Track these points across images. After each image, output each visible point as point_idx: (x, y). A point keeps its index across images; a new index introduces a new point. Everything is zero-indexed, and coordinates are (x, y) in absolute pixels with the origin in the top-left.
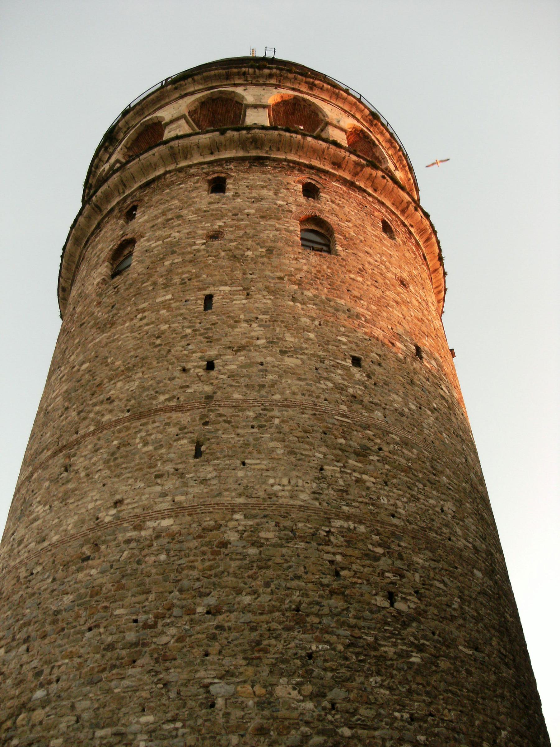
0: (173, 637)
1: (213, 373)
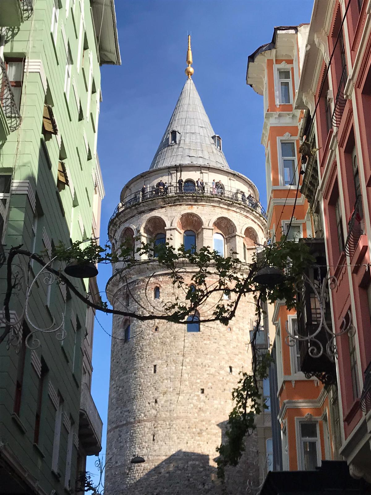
1: (157, 405)
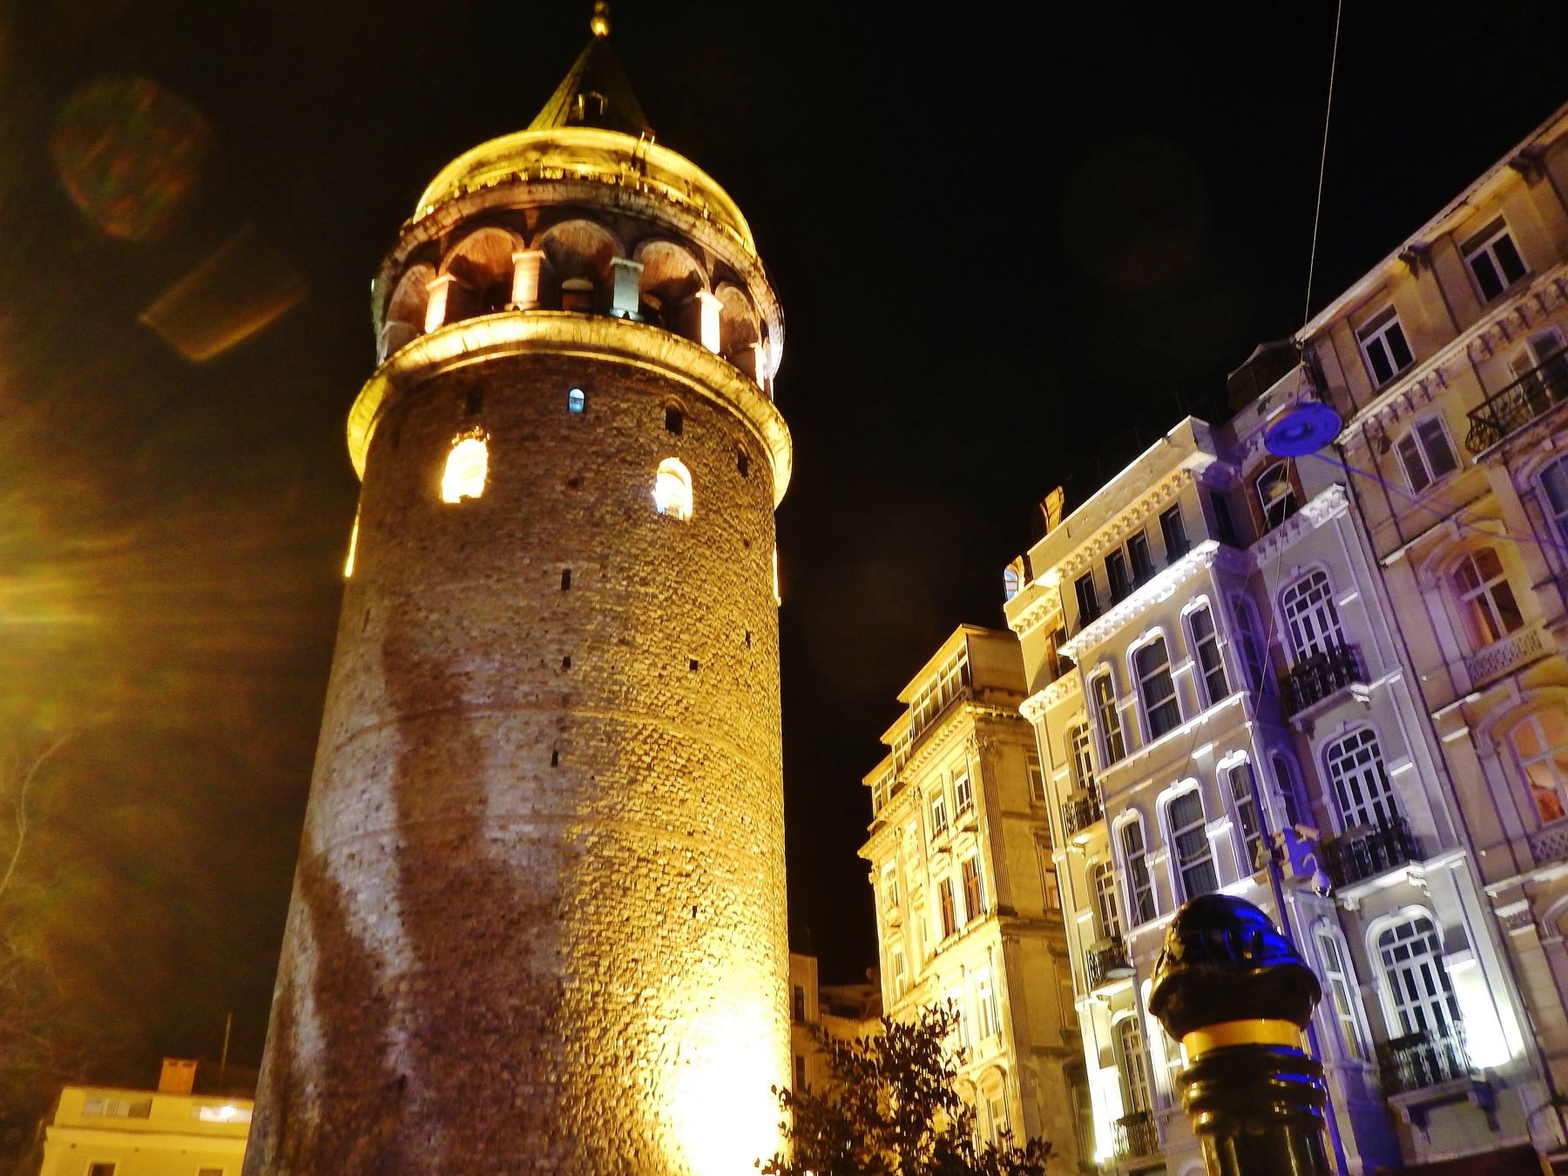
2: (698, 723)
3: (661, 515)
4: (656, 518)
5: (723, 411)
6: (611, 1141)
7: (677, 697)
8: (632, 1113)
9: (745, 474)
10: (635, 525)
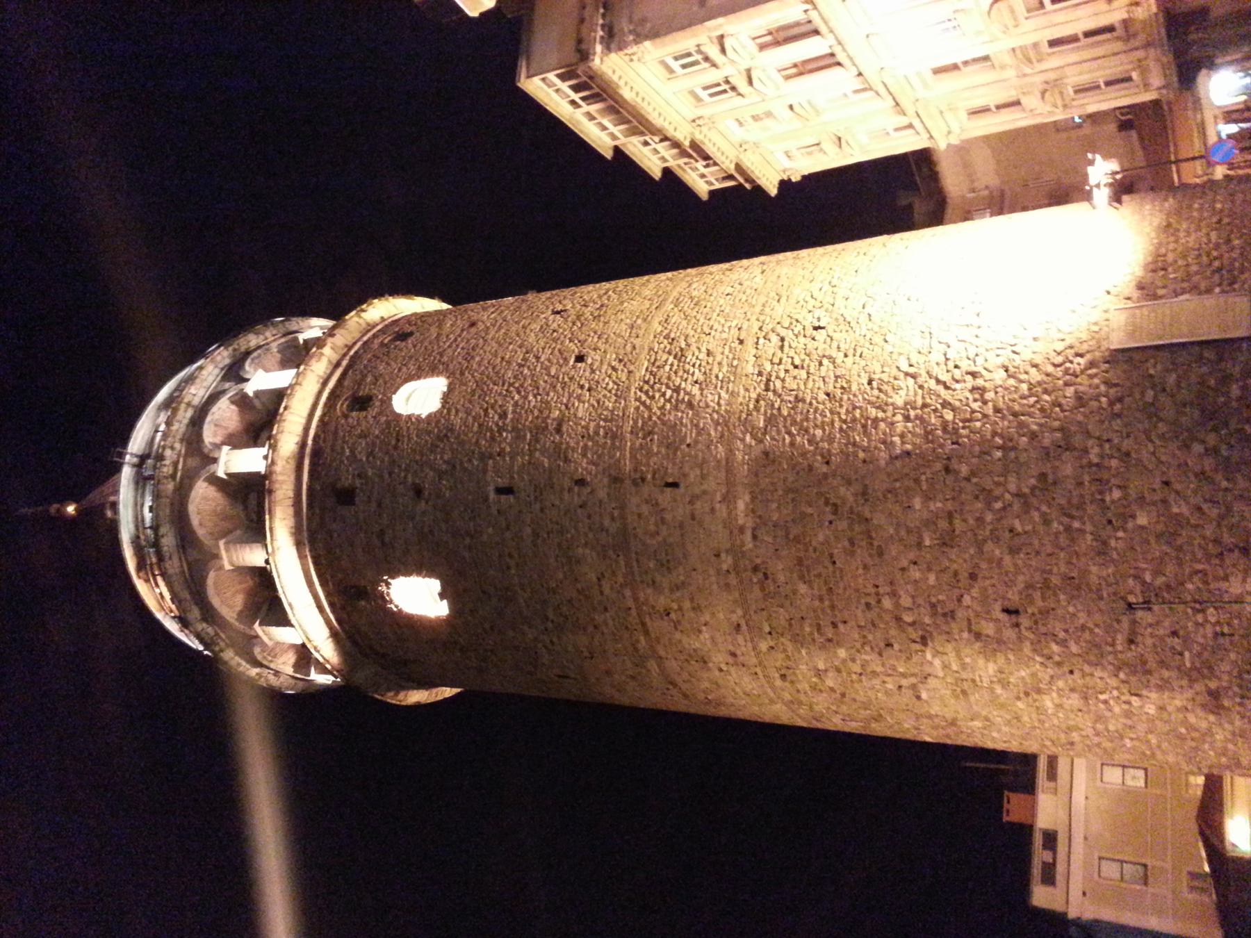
0: (848, 489)
2: (634, 348)
3: (443, 407)
4: (445, 411)
5: (354, 360)
6: (1067, 384)
7: (609, 372)
8: (1035, 366)
9: (411, 334)
10: (452, 430)
